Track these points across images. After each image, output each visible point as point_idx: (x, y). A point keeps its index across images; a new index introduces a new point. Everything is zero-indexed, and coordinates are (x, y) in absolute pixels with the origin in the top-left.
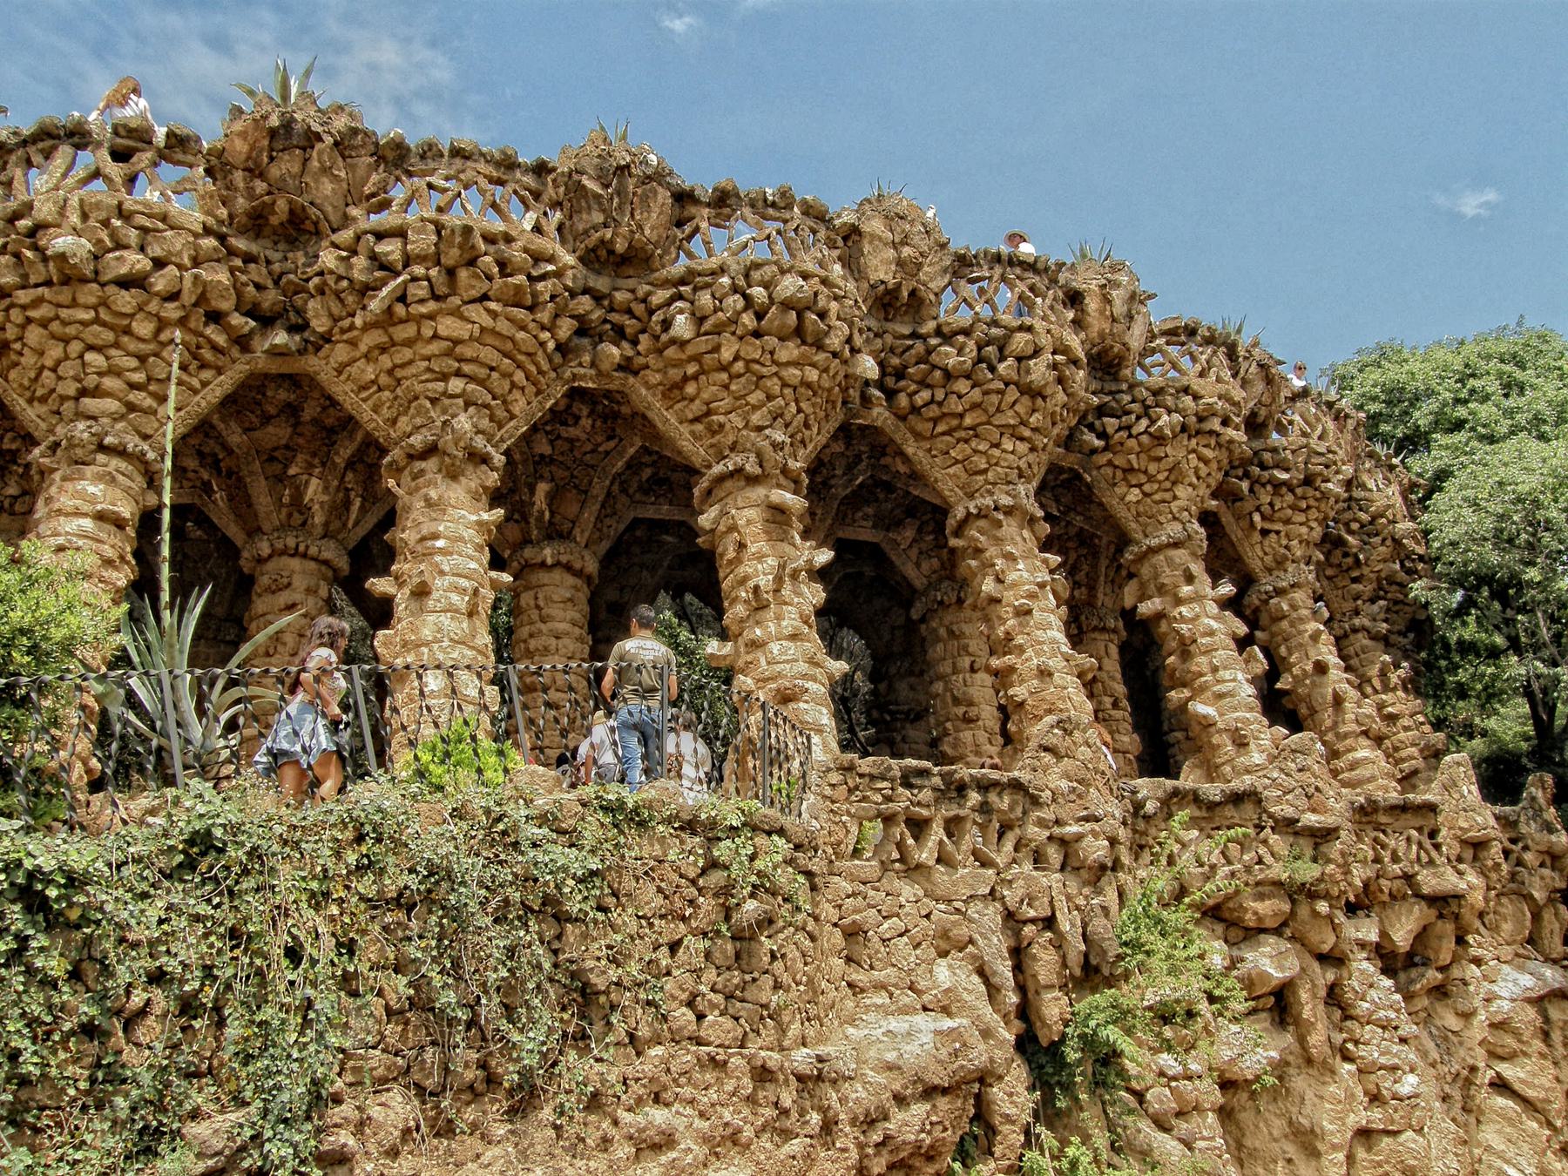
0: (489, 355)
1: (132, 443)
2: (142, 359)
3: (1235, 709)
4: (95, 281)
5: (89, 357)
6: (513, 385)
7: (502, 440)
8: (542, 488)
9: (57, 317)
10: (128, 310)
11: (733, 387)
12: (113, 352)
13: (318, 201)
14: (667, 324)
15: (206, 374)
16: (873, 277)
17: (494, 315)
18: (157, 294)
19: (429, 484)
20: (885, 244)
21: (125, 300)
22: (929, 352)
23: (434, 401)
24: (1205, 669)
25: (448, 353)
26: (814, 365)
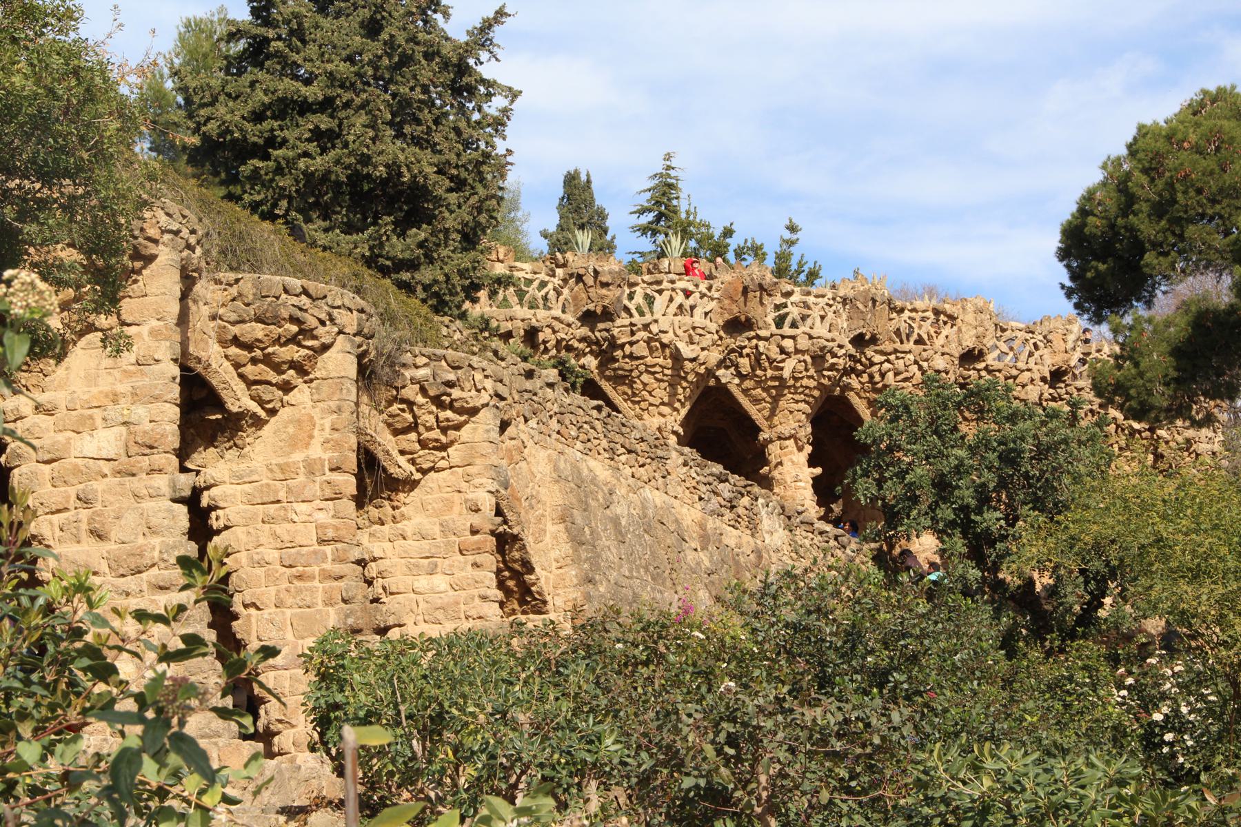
19: (791, 453)
23: (791, 412)
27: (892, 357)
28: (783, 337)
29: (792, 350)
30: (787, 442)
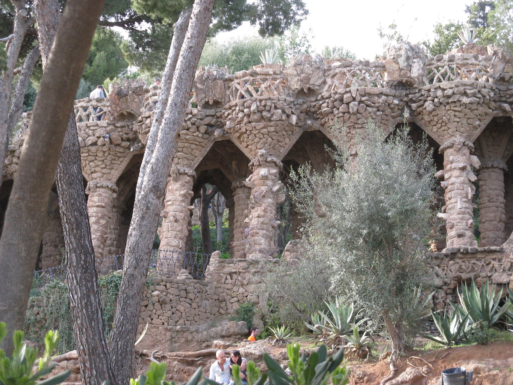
1: (105, 184)
4: (85, 146)
5: (91, 164)
6: (192, 149)
7: (194, 164)
8: (234, 163)
10: (95, 151)
12: (95, 161)
15: (121, 159)
16: (293, 88)
20: (295, 76)
21: (93, 149)
26: (271, 126)
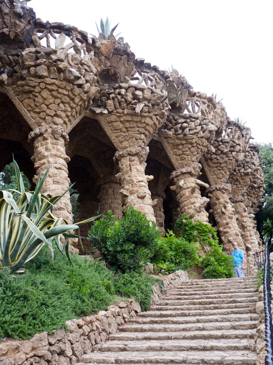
0: (151, 130)
2: (72, 108)
3: (255, 247)
5: (61, 105)
9: (57, 90)
11: (192, 149)
12: (67, 105)
13: (120, 72)
14: (183, 129)
17: (157, 119)
18: (84, 91)
19: (136, 164)
21: (77, 90)
22: (220, 145)
23: (136, 139)
24: (249, 235)
25: (144, 127)
27: (188, 120)
28: (136, 89)
29: (141, 97)
30: (133, 158)
